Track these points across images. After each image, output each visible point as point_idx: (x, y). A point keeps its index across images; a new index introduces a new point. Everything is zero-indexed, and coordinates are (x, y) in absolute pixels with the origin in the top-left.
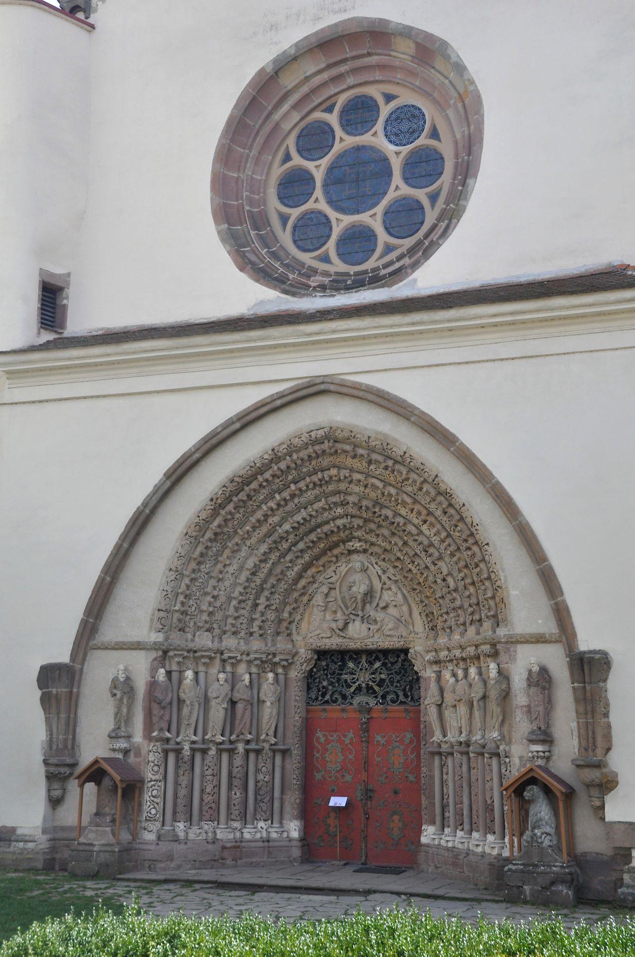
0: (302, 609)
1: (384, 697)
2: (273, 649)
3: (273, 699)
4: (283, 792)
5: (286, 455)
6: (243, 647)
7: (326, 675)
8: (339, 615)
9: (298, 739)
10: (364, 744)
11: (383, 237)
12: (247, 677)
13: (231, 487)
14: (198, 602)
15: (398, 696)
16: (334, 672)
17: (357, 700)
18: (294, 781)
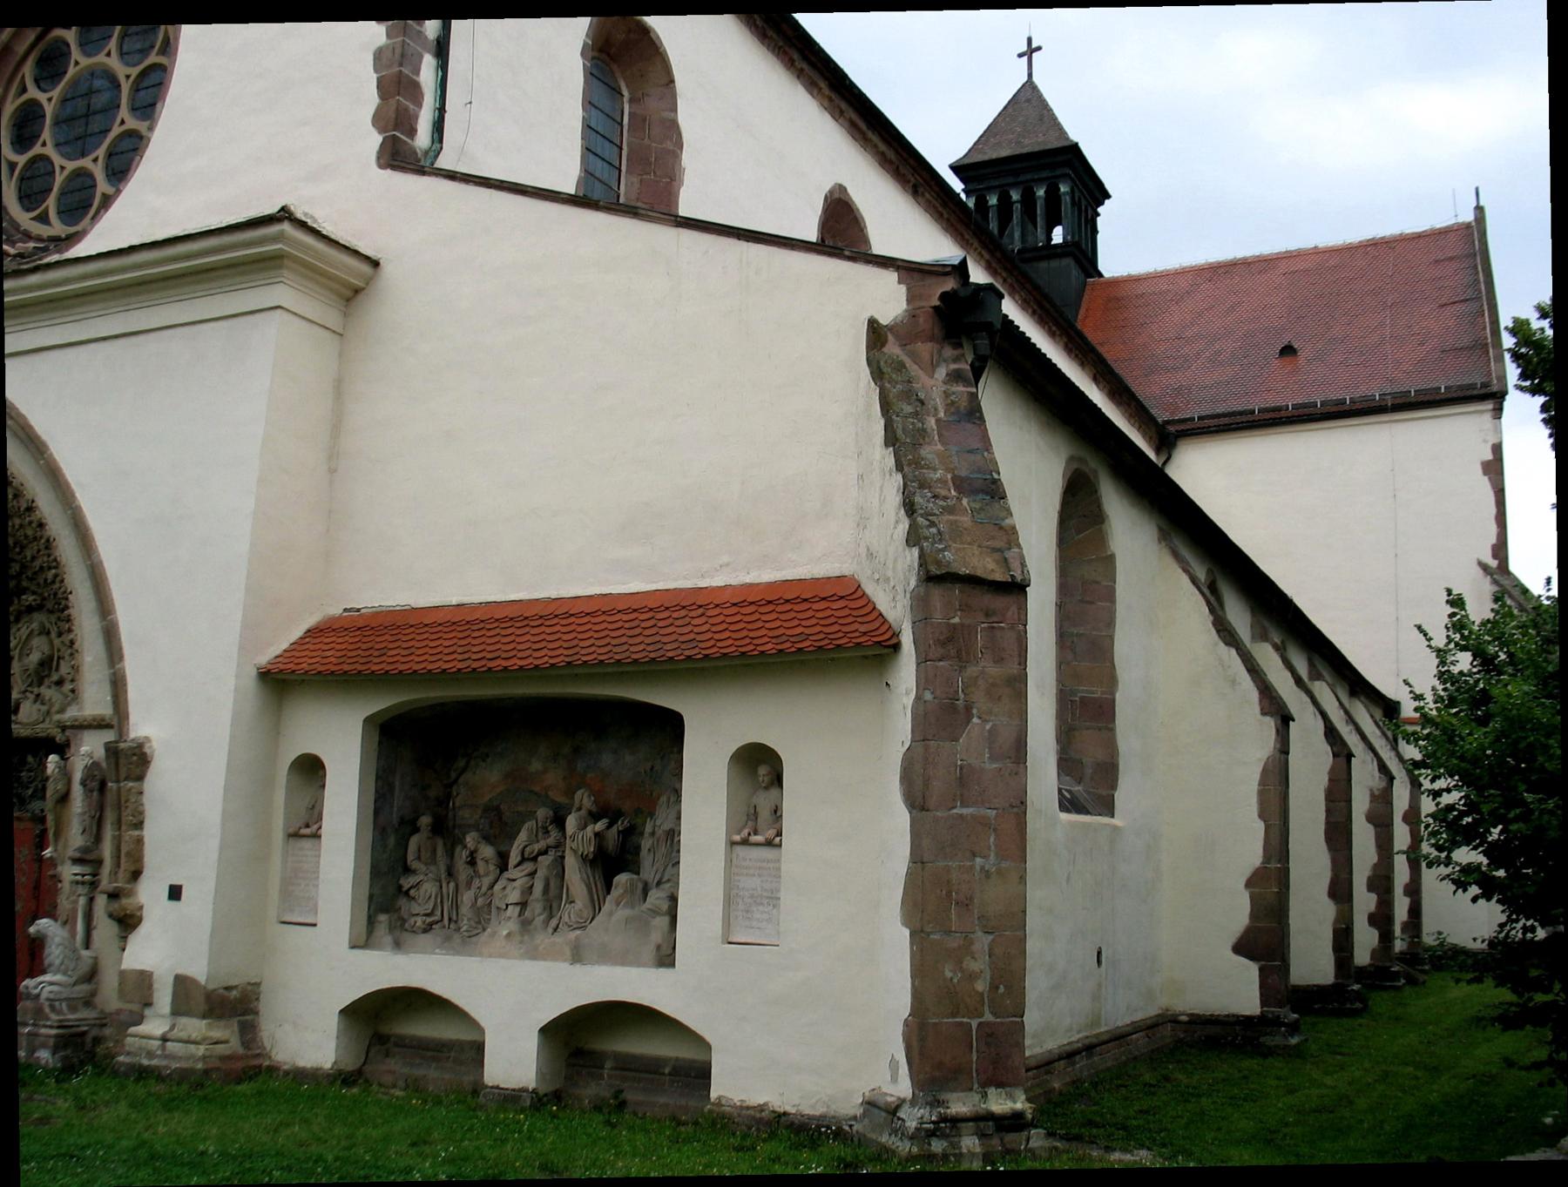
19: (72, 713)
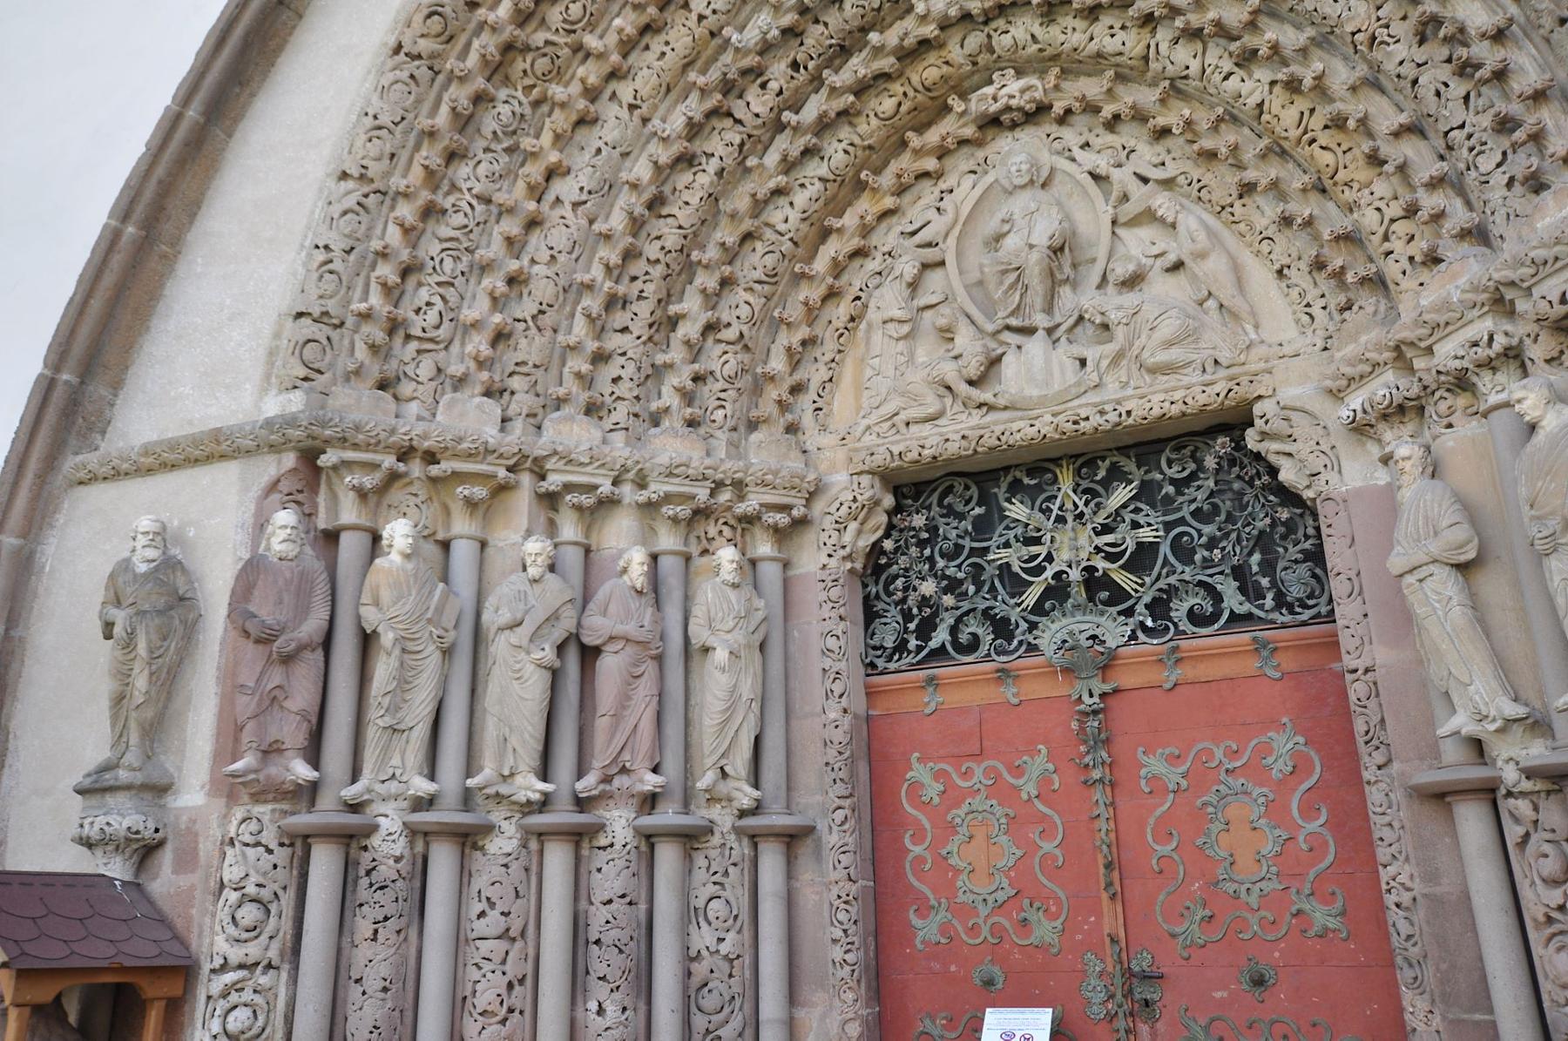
0: (829, 347)
1: (1159, 607)
2: (730, 468)
3: (738, 637)
4: (792, 997)
6: (619, 449)
7: (931, 559)
8: (965, 340)
9: (840, 789)
10: (1097, 794)
12: (637, 559)
14: (450, 293)
15: (1217, 598)
16: (959, 548)
17: (1051, 633)
18: (837, 953)
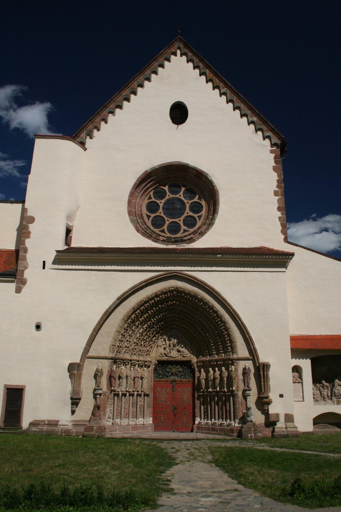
1: (181, 376)
5: (159, 295)
8: (167, 349)
11: (183, 227)
13: (140, 304)
17: (172, 378)
19: (235, 356)
